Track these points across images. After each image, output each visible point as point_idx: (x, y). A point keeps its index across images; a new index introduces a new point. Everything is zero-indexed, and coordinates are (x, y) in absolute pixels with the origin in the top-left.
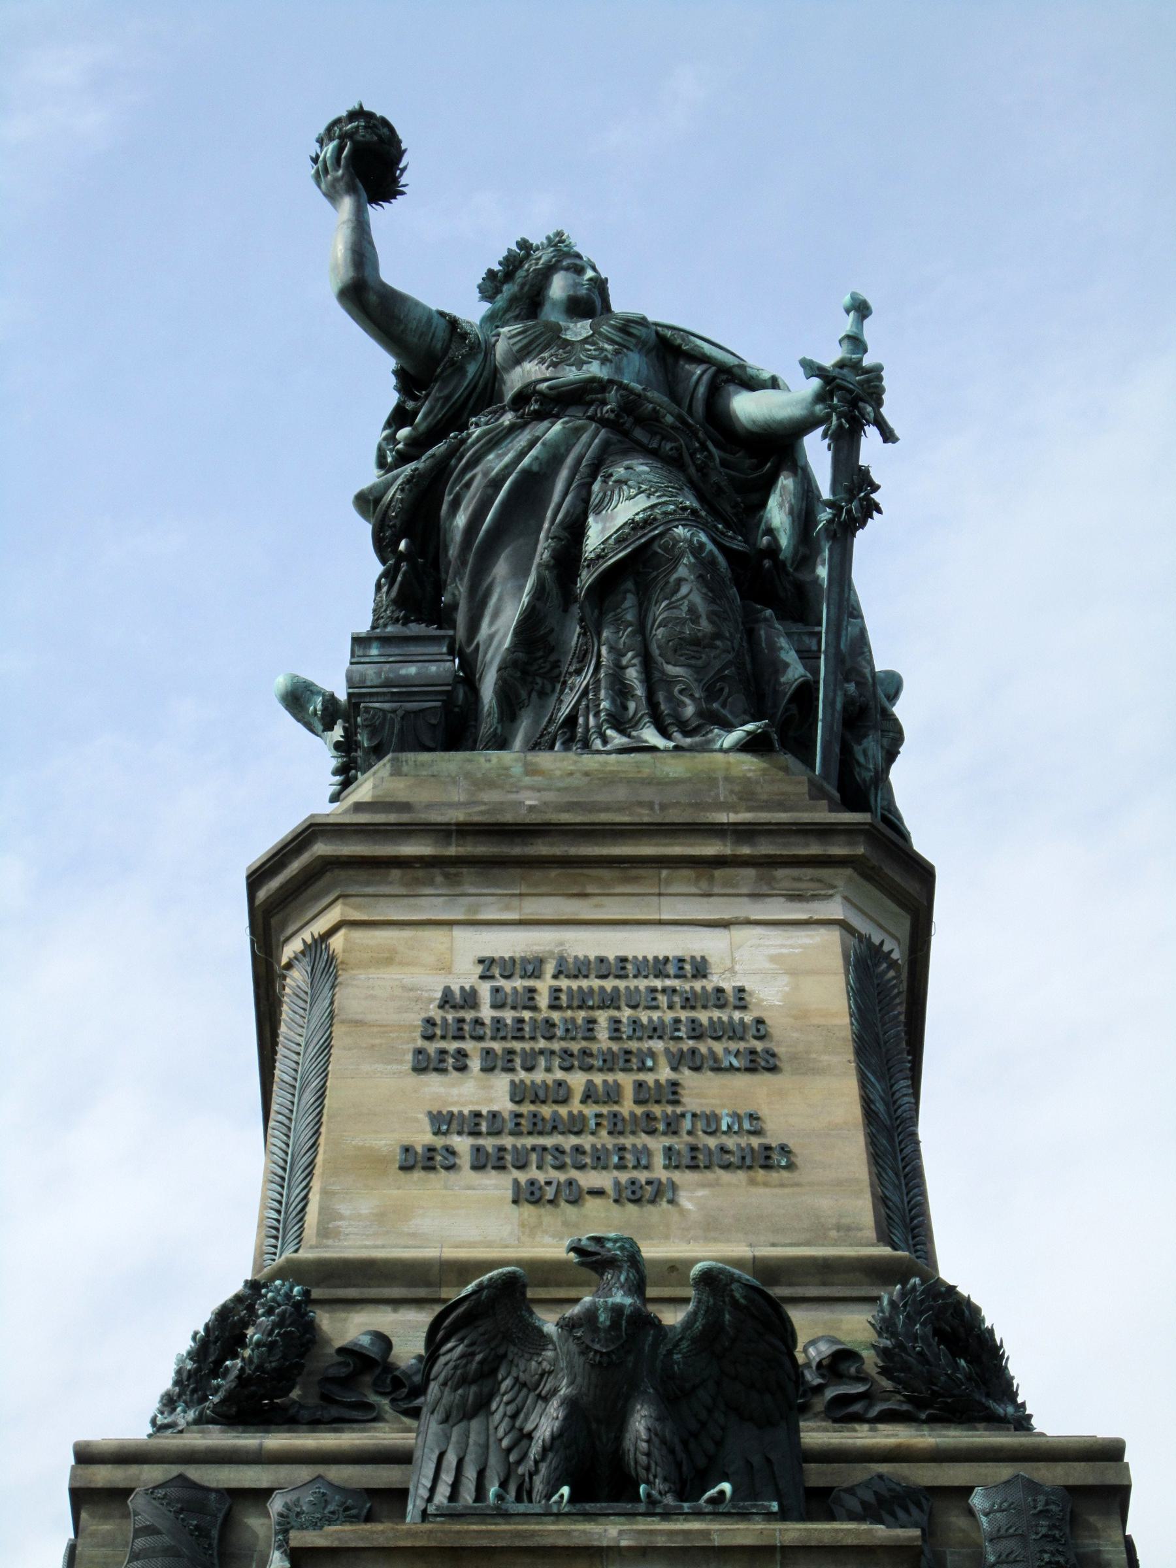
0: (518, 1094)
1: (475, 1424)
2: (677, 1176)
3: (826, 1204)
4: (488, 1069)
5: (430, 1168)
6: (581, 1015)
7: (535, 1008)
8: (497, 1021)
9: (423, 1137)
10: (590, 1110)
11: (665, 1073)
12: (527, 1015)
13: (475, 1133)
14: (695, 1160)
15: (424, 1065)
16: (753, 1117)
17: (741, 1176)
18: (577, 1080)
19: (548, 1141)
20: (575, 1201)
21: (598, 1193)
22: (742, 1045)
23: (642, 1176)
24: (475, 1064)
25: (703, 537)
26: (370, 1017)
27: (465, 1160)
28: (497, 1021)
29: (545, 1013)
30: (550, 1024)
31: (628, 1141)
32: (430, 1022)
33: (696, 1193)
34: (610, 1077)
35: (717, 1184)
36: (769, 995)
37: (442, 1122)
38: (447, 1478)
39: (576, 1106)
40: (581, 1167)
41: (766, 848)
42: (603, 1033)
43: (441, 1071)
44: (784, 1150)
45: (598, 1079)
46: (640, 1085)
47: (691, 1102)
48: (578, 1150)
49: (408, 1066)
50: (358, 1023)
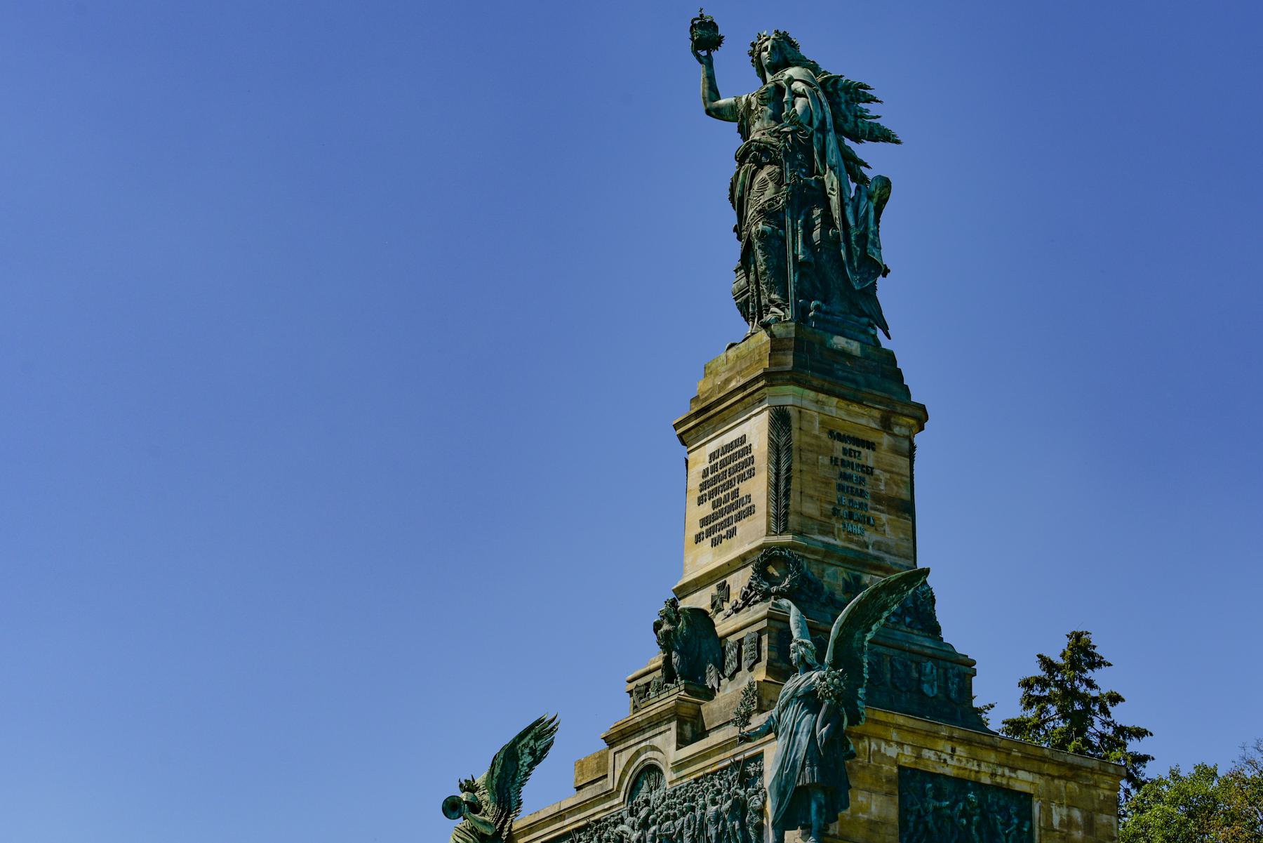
9: (699, 530)
14: (739, 518)
15: (701, 501)
25: (760, 226)
33: (742, 527)
36: (754, 447)
37: (704, 522)
41: (749, 391)
47: (742, 494)
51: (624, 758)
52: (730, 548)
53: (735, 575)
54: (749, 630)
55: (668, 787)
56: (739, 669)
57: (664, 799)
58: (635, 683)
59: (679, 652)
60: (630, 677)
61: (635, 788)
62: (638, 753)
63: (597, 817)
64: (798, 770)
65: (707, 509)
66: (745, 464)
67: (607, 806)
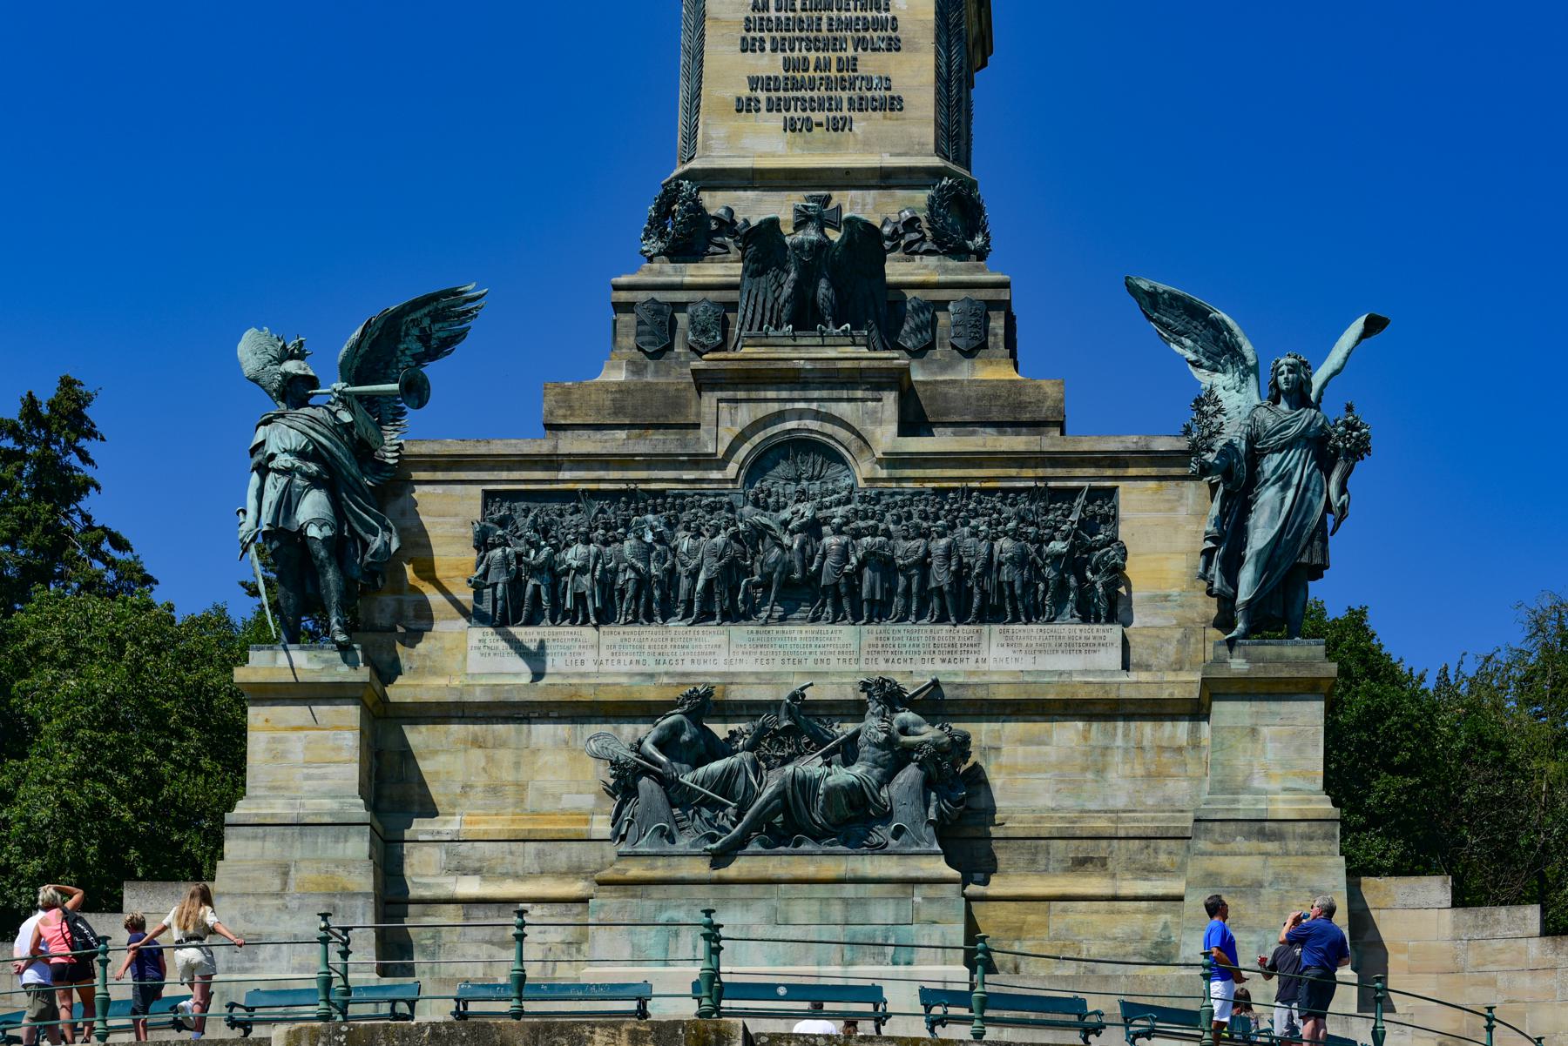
0: (788, 65)
1: (763, 279)
2: (852, 114)
3: (914, 130)
4: (774, 50)
5: (749, 111)
6: (816, 14)
7: (794, 11)
8: (778, 19)
9: (745, 92)
10: (818, 74)
11: (850, 52)
12: (791, 14)
13: (769, 90)
14: (860, 105)
15: (747, 46)
16: (887, 79)
17: (879, 114)
18: (812, 56)
19: (799, 94)
20: (809, 130)
21: (819, 125)
22: (884, 34)
23: (838, 114)
24: (768, 46)
26: (721, 16)
27: (763, 105)
28: (778, 19)
29: (799, 14)
30: (801, 21)
31: (833, 94)
32: (748, 19)
33: (862, 123)
34: (826, 54)
35: (869, 119)
38: (752, 301)
39: (811, 72)
40: (813, 110)
42: (824, 26)
43: (754, 51)
44: (900, 100)
45: (821, 55)
46: (840, 59)
47: (862, 71)
48: (812, 99)
49: (738, 48)
50: (716, 19)
51: (746, 415)
52: (836, 147)
53: (853, 193)
54: (962, 294)
55: (862, 484)
56: (932, 346)
57: (848, 501)
58: (641, 296)
59: (832, 283)
60: (624, 280)
61: (758, 467)
62: (780, 417)
63: (653, 486)
64: (1303, 541)
65: (769, 64)
66: (879, 25)
67: (687, 475)
